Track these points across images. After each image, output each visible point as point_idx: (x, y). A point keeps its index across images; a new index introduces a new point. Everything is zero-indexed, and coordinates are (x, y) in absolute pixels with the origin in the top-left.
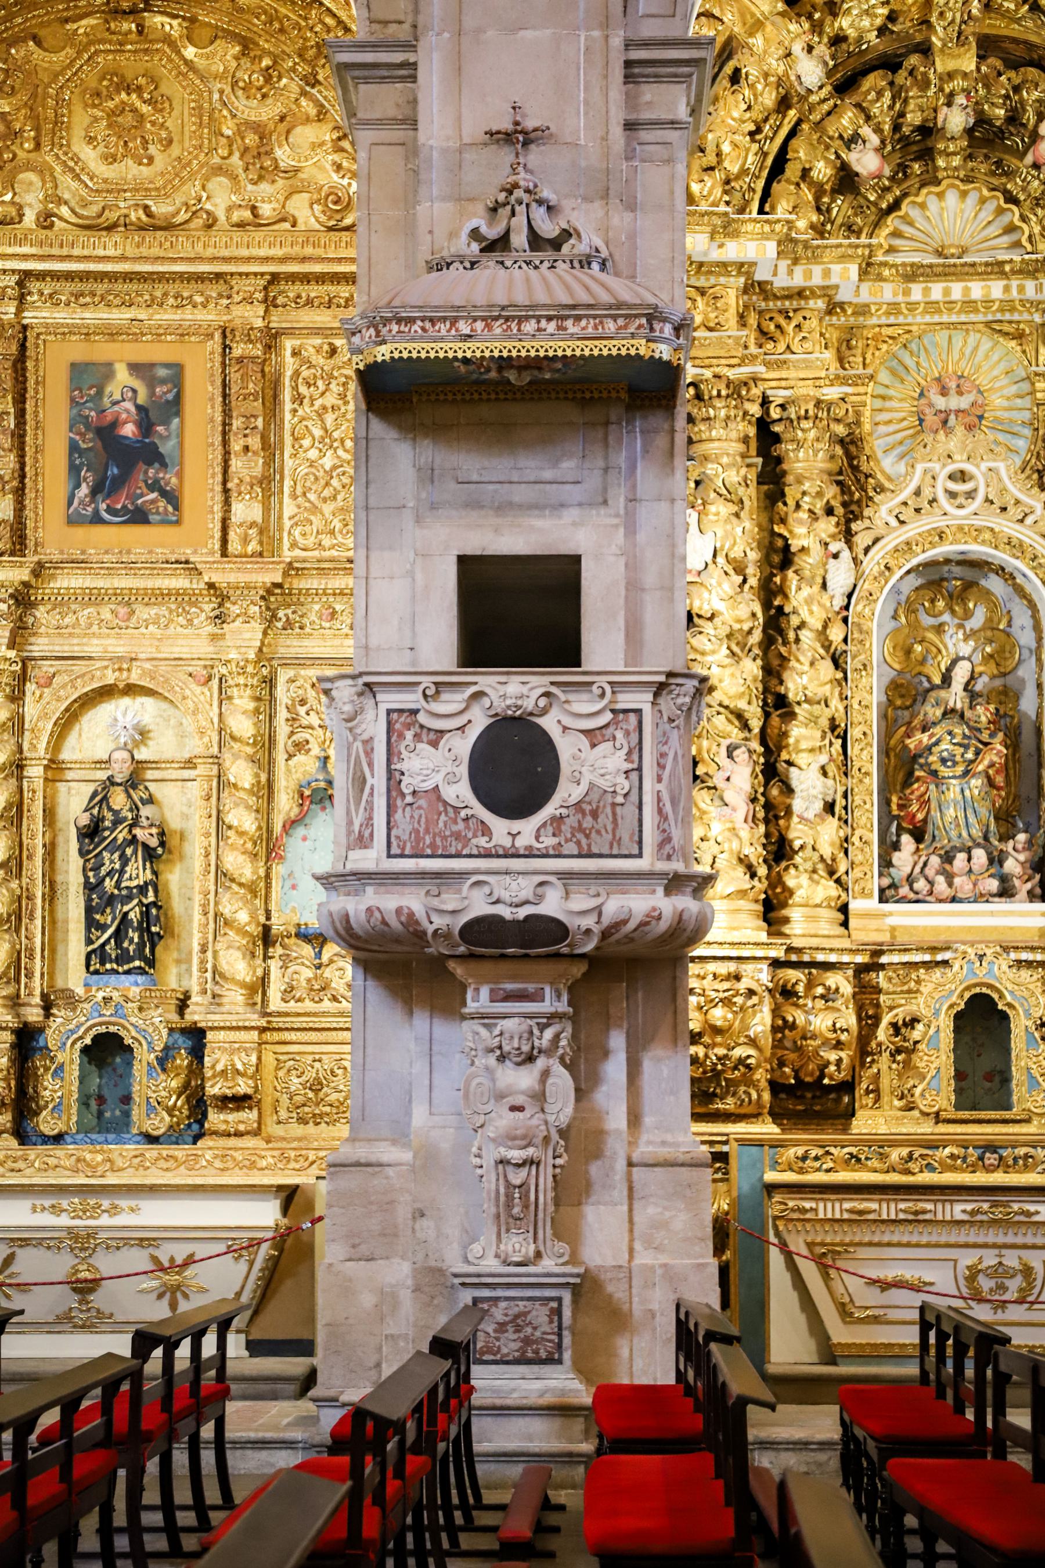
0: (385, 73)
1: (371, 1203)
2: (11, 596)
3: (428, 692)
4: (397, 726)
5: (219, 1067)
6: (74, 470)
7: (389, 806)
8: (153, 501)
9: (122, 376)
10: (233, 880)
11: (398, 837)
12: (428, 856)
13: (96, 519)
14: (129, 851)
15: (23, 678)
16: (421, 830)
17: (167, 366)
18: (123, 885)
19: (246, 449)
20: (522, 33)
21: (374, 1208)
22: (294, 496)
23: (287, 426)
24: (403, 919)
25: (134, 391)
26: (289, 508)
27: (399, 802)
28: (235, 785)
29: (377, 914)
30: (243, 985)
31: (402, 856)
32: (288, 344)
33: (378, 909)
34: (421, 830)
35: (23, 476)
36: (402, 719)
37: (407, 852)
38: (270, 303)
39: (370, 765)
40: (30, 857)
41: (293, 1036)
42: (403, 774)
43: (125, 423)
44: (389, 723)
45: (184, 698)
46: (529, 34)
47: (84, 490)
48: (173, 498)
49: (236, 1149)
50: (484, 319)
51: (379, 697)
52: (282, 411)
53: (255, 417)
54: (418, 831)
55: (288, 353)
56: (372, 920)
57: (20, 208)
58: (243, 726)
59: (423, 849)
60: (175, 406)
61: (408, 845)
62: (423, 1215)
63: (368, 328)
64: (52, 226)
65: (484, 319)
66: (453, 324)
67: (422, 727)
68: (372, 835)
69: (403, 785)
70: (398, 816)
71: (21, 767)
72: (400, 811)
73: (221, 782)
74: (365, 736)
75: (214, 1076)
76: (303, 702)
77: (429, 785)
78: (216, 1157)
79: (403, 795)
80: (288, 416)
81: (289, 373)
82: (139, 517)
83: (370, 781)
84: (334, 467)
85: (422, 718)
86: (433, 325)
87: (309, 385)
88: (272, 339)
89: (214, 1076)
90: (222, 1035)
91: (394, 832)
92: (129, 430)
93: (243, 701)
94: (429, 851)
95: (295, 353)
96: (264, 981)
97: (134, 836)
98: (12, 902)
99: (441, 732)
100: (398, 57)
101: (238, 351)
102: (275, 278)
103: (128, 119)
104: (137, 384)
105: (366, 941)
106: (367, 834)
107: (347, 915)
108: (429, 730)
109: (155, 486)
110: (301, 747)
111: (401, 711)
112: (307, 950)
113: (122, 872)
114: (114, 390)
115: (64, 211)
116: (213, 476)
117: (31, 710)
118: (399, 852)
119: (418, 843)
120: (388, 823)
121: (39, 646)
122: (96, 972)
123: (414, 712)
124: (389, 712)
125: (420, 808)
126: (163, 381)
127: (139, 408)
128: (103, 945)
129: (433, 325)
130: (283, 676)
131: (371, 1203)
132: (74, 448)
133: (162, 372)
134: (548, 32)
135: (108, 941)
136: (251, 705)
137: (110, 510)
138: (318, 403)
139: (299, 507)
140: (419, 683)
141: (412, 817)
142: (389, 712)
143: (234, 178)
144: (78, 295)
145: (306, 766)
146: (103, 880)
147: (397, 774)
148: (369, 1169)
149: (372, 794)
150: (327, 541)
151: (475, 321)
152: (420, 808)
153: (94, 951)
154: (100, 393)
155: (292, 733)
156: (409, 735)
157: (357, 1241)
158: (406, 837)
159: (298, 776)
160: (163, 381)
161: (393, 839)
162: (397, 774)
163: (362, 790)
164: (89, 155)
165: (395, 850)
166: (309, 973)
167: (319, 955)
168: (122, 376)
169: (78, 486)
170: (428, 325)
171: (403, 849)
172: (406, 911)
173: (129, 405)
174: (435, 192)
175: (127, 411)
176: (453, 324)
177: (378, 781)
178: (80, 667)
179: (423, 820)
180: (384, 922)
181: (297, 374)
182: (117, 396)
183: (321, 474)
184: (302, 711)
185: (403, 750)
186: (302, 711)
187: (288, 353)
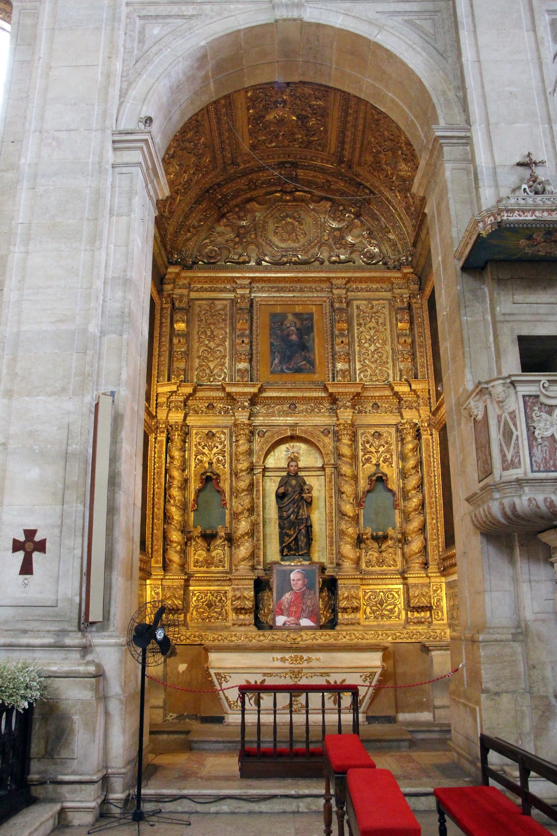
0: (455, 141)
1: (505, 661)
2: (249, 400)
3: (545, 385)
4: (529, 404)
5: (346, 595)
6: (272, 353)
7: (529, 445)
8: (304, 365)
9: (290, 317)
10: (346, 515)
11: (535, 461)
12: (553, 471)
13: (282, 371)
14: (300, 504)
15: (252, 433)
16: (548, 458)
17: (308, 314)
18: (299, 517)
19: (342, 342)
20: (515, 125)
21: (506, 664)
22: (360, 361)
23: (356, 335)
24: (548, 504)
25: (295, 323)
26: (358, 366)
27: (534, 443)
28: (345, 475)
29: (534, 502)
30: (351, 560)
31: (539, 471)
32: (355, 303)
33: (534, 499)
34: (548, 458)
35: (252, 355)
36: (531, 400)
37: (541, 469)
38: (348, 290)
39: (515, 425)
40: (257, 507)
41: (371, 582)
42: (535, 428)
43: (292, 335)
44: (525, 403)
45: (319, 441)
46: (518, 125)
47: (277, 361)
48: (312, 363)
49: (343, 631)
50: (547, 210)
51: (518, 389)
52: (354, 329)
53: (344, 330)
54: (545, 459)
55: (355, 307)
56: (531, 505)
57: (249, 257)
58: (346, 450)
59: (550, 468)
60: (310, 330)
61: (542, 466)
62: (534, 667)
63: (489, 217)
64: (261, 264)
65: (547, 210)
66: (533, 213)
67: (541, 404)
68: (519, 461)
69: (536, 433)
70: (535, 450)
71: (252, 470)
72: (535, 448)
73: (340, 475)
74: (511, 410)
75: (343, 599)
76: (368, 442)
77: (548, 434)
78: (347, 634)
79: (536, 439)
80: (356, 331)
81: (355, 314)
82: (299, 370)
83: (515, 433)
84: (375, 350)
85: (543, 399)
86: (524, 213)
87: (363, 320)
88: (348, 303)
89: (343, 599)
90: (346, 582)
91: (533, 459)
92: (294, 337)
93: (346, 440)
94: (553, 469)
95: (358, 307)
96: (359, 558)
97: (303, 497)
98: (251, 526)
99: (551, 406)
100: (462, 134)
101: (337, 305)
102: (349, 280)
103: (290, 227)
104: (296, 321)
105: (523, 518)
106: (516, 461)
107: (514, 504)
108: (546, 405)
109: (305, 359)
110: (368, 460)
111: (530, 396)
112: (376, 545)
113: (298, 512)
114: (287, 323)
115: (267, 259)
116: (328, 353)
117: (256, 447)
118: (537, 469)
119: (546, 465)
120: (530, 454)
121: (259, 421)
122: (287, 555)
123: (537, 397)
124: (524, 396)
125: (545, 446)
126: (306, 319)
127: (297, 329)
128: (290, 543)
129: (524, 213)
130: (360, 432)
131: (505, 661)
132: (272, 345)
133: (306, 316)
134: (527, 125)
135: (292, 542)
136: (350, 442)
137: (288, 369)
138: (367, 326)
139: (362, 365)
140: (540, 381)
141: (542, 451)
142: (524, 396)
143: (330, 247)
144: (272, 288)
145: (370, 468)
146: (290, 516)
147: (532, 428)
148: (502, 643)
149: (517, 439)
150: (374, 379)
151: (543, 212)
152: (545, 446)
153: (285, 546)
154: (282, 324)
155: (365, 455)
156: (536, 408)
157: (499, 682)
158: (539, 461)
159: (368, 473)
160: (306, 319)
161: (533, 462)
162: (532, 428)
163: (511, 439)
164: (275, 240)
165: (535, 468)
166: (376, 555)
167: (380, 547)
168: (290, 317)
169: (274, 359)
170: (521, 213)
171: (539, 468)
172: (549, 500)
173: (292, 328)
174: (486, 184)
175: (292, 330)
176: (533, 213)
177: (521, 432)
178: (276, 429)
179: (548, 452)
180: (537, 506)
181: (358, 315)
182: (288, 325)
183: (370, 353)
184: (368, 446)
185: (534, 416)
186: (368, 446)
187: (355, 307)
